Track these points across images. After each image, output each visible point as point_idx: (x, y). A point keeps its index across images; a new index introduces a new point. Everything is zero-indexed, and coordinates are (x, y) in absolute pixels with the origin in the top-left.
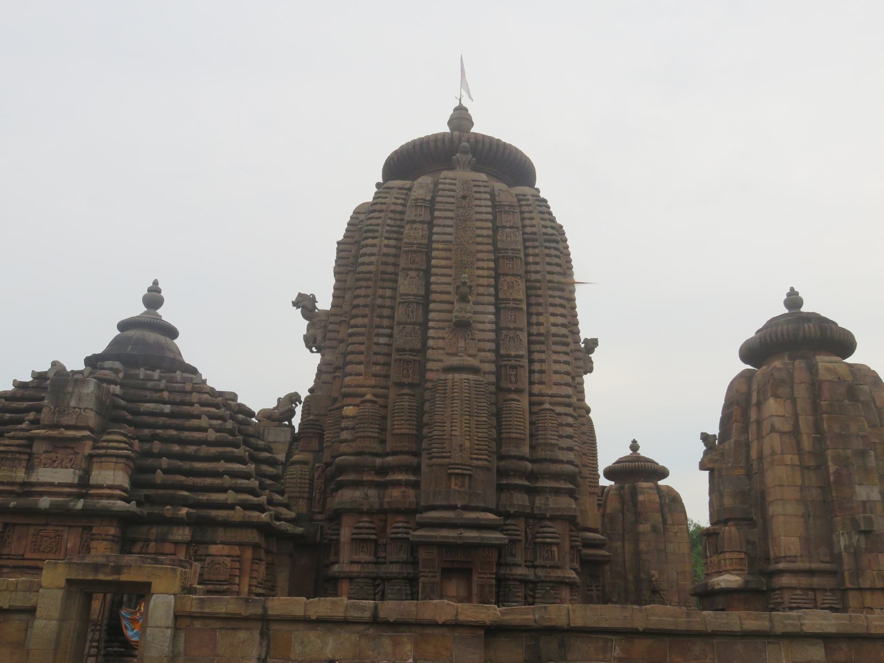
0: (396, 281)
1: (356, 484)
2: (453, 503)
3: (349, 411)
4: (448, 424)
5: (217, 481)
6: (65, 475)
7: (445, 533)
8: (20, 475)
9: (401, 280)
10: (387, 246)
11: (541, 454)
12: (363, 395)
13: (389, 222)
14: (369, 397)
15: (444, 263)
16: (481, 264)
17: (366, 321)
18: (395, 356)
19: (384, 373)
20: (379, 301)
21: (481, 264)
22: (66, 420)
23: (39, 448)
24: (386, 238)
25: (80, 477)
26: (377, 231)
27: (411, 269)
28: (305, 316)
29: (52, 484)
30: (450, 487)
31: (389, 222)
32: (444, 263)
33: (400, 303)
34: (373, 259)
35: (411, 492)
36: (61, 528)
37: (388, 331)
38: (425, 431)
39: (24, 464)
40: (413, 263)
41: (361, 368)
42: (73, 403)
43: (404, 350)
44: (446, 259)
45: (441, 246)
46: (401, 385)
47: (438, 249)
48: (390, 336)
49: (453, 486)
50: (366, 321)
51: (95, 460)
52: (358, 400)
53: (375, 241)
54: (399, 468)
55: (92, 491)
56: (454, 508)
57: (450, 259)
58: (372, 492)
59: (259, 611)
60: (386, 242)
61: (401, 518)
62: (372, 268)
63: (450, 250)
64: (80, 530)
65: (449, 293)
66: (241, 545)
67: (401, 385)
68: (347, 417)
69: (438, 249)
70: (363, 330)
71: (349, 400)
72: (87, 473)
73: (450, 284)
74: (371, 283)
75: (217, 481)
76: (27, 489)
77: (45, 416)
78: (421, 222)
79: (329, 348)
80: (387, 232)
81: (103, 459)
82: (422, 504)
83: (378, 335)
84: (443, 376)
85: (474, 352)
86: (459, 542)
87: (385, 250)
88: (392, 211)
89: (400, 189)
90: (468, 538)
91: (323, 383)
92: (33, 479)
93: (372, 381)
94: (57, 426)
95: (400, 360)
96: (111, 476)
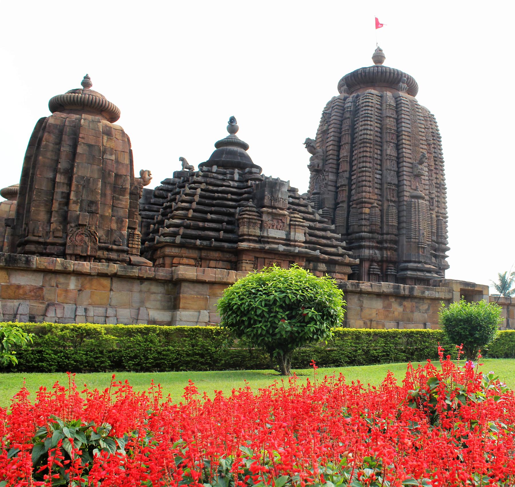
0: (381, 146)
1: (369, 247)
2: (421, 260)
3: (367, 211)
4: (417, 224)
5: (329, 242)
6: (281, 234)
7: (419, 273)
8: (258, 232)
9: (385, 147)
10: (376, 127)
11: (440, 240)
12: (371, 203)
13: (376, 114)
14: (375, 205)
15: (408, 142)
16: (421, 146)
17: (371, 165)
18: (385, 186)
19: (379, 193)
20: (376, 156)
21: (421, 146)
22: (277, 205)
23: (265, 218)
24: (376, 122)
25: (287, 235)
26: (372, 118)
27: (391, 142)
28: (310, 151)
29: (275, 238)
30: (419, 253)
31: (376, 114)
32: (408, 142)
33: (387, 159)
34: (372, 133)
35: (395, 253)
36: (279, 261)
37: (380, 172)
38: (404, 225)
39: (259, 226)
40: (392, 139)
41: (371, 190)
42: (280, 196)
43: (391, 184)
44: (408, 140)
45: (406, 134)
46: (391, 201)
47: (405, 135)
48: (381, 175)
49: (421, 253)
50: (371, 165)
51: (292, 227)
52: (370, 206)
53: (372, 123)
54: (391, 241)
55: (292, 243)
56: (419, 262)
57: (410, 141)
58: (377, 252)
59: (509, 302)
60: (376, 124)
61: (391, 265)
62: (371, 137)
63: (410, 136)
64: (288, 262)
65: (410, 158)
66: (344, 274)
67: (391, 201)
68: (365, 213)
69: (405, 135)
70: (370, 170)
71: (366, 205)
72: (288, 234)
73: (410, 154)
74: (372, 146)
75: (329, 242)
76: (260, 240)
77: (266, 202)
78: (393, 118)
79: (331, 172)
80: (376, 119)
81: (296, 227)
82: (404, 259)
83: (376, 173)
84: (413, 200)
85: (422, 190)
86: (425, 278)
87: (376, 129)
88: (377, 108)
89: (377, 96)
90: (429, 276)
91: (329, 191)
92: (265, 234)
93: (376, 197)
94: (276, 208)
95: (390, 188)
96: (300, 236)
